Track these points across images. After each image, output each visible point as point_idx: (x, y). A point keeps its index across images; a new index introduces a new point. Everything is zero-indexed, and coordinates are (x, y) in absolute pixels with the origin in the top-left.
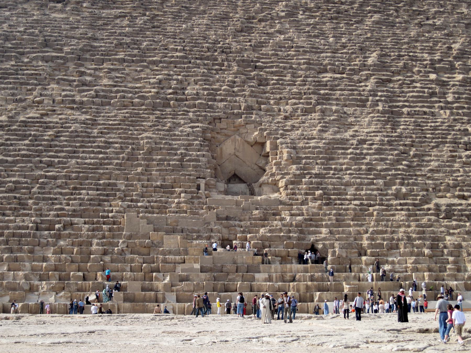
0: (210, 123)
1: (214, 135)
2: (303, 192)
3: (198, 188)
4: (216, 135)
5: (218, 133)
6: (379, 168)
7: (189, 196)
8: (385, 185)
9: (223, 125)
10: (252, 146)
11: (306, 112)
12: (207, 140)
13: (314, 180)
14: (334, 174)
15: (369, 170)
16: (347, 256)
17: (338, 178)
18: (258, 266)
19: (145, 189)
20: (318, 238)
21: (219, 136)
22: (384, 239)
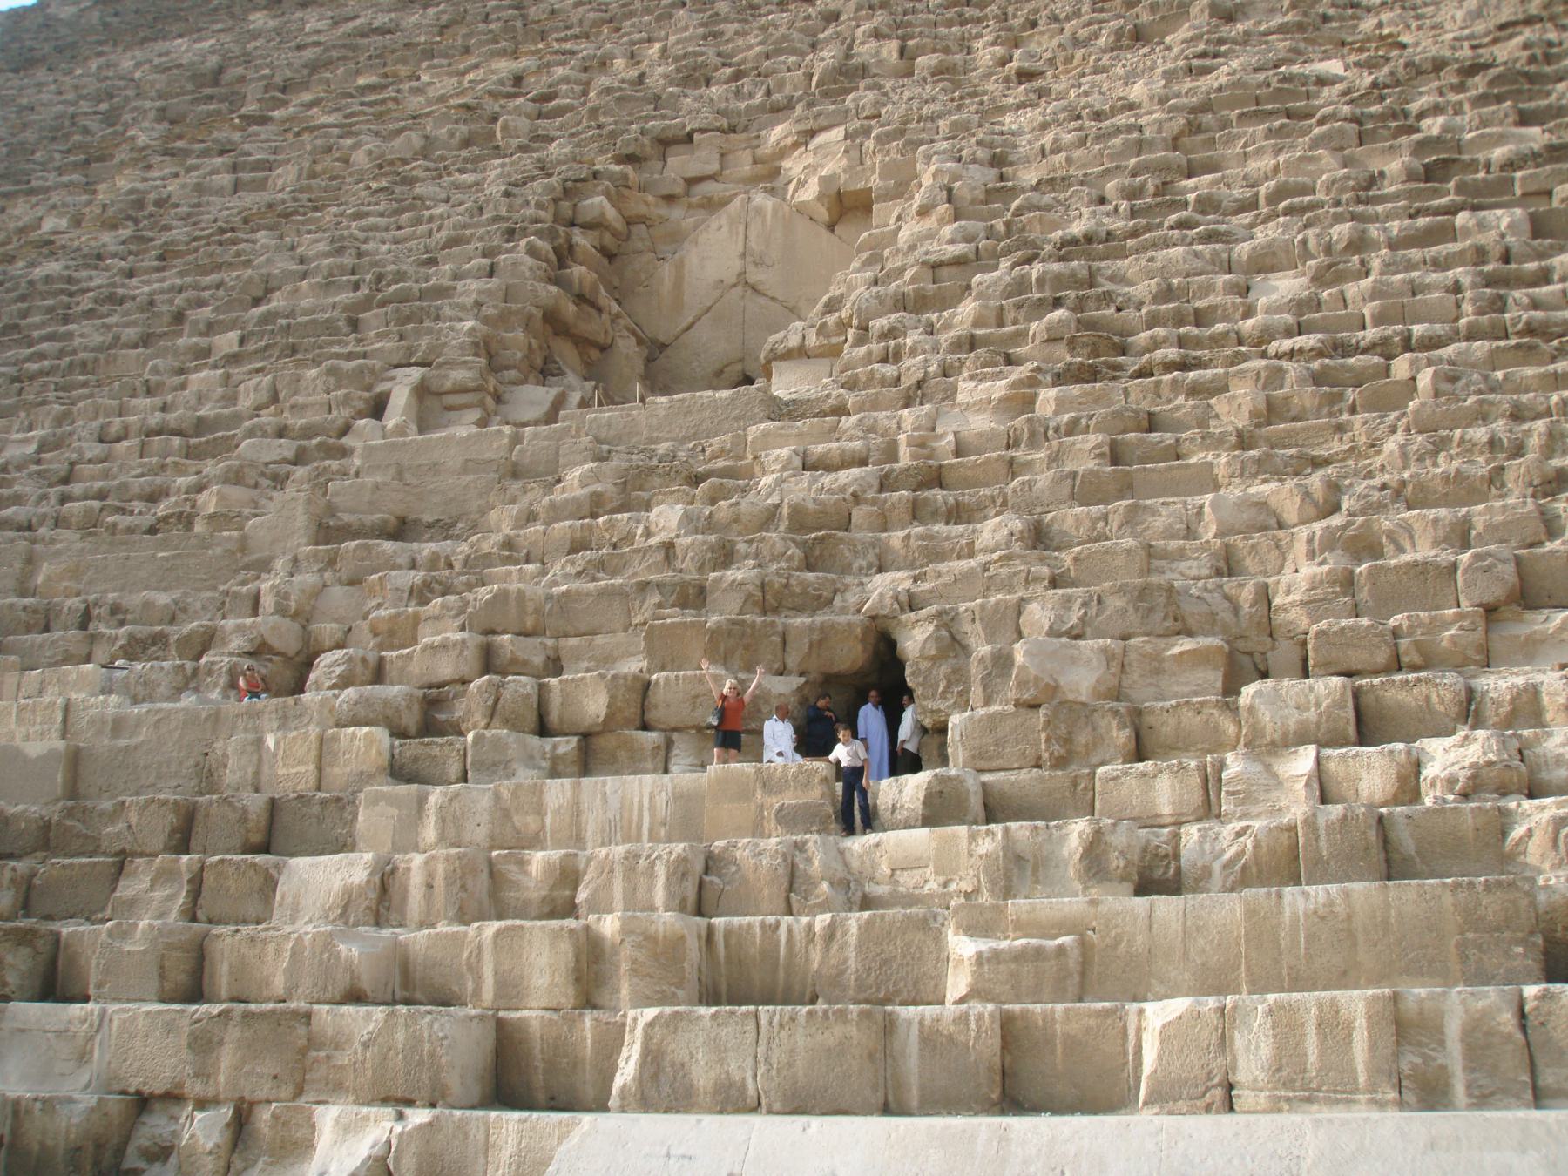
0: (630, 159)
1: (643, 210)
2: (945, 338)
3: (377, 408)
4: (663, 211)
5: (670, 199)
6: (1498, 153)
7: (287, 447)
8: (1536, 234)
9: (699, 160)
10: (831, 227)
11: (1139, 36)
12: (587, 227)
13: (1036, 269)
14: (1182, 225)
15: (1433, 174)
16: (1117, 694)
17: (1209, 237)
18: (343, 805)
19: (98, 449)
20: (924, 586)
21: (676, 213)
22: (1461, 536)
